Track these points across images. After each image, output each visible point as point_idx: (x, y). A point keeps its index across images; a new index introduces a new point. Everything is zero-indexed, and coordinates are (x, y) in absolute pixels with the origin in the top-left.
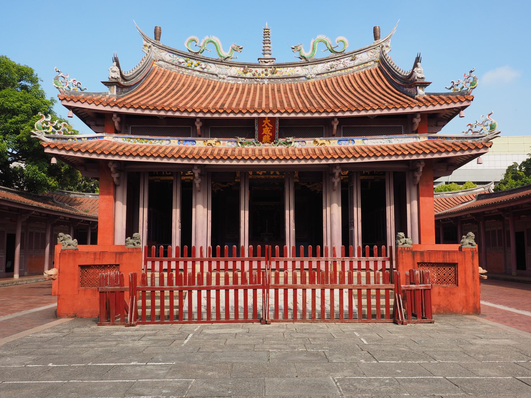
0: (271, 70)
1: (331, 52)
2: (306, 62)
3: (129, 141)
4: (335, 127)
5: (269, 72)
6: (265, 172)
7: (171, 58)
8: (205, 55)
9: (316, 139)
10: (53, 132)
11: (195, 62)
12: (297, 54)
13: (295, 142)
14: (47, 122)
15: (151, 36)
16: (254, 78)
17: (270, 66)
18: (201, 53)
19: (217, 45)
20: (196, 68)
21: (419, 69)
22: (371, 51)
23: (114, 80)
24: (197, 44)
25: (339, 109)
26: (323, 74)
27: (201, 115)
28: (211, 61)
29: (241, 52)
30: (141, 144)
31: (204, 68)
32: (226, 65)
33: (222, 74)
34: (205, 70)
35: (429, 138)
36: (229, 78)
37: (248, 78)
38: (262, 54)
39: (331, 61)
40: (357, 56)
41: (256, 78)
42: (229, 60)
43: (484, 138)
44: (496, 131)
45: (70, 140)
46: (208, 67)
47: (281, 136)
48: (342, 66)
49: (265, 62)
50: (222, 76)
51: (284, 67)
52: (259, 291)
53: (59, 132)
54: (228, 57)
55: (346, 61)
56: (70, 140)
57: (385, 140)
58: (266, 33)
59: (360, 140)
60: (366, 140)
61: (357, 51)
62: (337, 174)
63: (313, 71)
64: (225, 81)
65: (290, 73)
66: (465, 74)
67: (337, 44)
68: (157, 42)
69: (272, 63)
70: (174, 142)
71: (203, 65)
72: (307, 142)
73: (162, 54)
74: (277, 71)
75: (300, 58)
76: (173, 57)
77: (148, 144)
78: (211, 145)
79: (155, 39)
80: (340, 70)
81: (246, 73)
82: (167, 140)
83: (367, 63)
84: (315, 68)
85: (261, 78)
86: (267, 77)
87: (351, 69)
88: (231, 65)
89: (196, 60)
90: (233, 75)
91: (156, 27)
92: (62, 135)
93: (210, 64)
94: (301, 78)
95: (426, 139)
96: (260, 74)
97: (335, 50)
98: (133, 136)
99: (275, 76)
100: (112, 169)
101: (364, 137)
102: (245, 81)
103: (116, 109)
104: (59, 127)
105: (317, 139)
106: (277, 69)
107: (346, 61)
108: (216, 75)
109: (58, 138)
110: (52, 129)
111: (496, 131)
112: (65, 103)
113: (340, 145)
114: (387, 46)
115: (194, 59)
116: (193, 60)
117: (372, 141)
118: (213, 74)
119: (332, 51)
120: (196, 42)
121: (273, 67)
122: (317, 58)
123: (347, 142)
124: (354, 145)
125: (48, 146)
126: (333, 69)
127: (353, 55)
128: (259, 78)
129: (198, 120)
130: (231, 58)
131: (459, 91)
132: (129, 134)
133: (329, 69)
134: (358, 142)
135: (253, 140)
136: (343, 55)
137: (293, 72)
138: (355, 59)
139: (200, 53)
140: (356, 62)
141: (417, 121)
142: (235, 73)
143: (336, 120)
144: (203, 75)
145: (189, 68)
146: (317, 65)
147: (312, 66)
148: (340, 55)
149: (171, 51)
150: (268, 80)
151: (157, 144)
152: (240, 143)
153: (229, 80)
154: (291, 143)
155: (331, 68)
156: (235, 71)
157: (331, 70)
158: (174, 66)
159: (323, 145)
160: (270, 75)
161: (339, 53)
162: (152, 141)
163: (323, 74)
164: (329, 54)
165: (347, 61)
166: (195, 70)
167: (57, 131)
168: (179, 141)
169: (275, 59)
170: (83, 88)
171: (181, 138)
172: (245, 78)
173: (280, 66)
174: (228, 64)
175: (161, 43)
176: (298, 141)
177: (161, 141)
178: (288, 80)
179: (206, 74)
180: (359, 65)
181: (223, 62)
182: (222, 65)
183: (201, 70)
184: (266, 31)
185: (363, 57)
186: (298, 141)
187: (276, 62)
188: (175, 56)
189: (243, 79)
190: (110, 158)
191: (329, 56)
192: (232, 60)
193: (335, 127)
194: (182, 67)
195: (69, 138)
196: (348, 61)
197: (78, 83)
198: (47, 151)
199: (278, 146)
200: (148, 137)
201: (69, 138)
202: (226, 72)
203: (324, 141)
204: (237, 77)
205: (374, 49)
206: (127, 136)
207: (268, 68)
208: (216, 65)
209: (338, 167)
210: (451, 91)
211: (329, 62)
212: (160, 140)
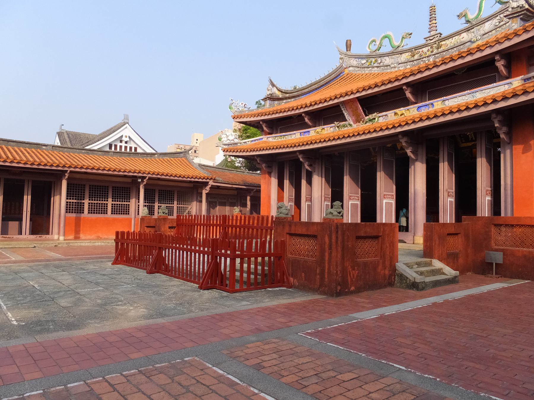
1: (500, 4)
2: (471, 26)
3: (275, 139)
6: (377, 150)
7: (357, 63)
8: (383, 51)
9: (395, 110)
11: (373, 60)
12: (463, 20)
13: (379, 117)
15: (344, 49)
17: (435, 43)
18: (378, 50)
19: (389, 38)
28: (385, 55)
29: (410, 37)
31: (380, 63)
32: (397, 54)
33: (393, 64)
37: (416, 60)
42: (400, 49)
46: (383, 60)
47: (366, 116)
49: (429, 39)
50: (393, 66)
56: (239, 144)
57: (469, 96)
58: (433, 11)
60: (447, 101)
63: (479, 33)
65: (455, 42)
68: (349, 53)
69: (437, 38)
72: (389, 115)
73: (351, 61)
74: (442, 45)
75: (466, 23)
76: (358, 61)
77: (285, 139)
81: (413, 56)
84: (482, 29)
85: (428, 57)
86: (433, 53)
88: (401, 53)
89: (374, 57)
90: (403, 62)
91: (347, 41)
93: (385, 58)
98: (276, 135)
101: (445, 98)
103: (259, 118)
105: (397, 111)
106: (443, 43)
108: (389, 65)
112: (238, 120)
115: (373, 57)
116: (372, 59)
118: (387, 66)
120: (375, 42)
121: (437, 42)
122: (484, 17)
123: (427, 107)
124: (435, 108)
126: (502, 23)
128: (425, 57)
130: (402, 46)
133: (497, 24)
134: (438, 105)
139: (377, 51)
141: (500, 64)
142: (405, 59)
144: (380, 69)
145: (370, 66)
150: (434, 56)
152: (338, 127)
154: (375, 119)
155: (500, 22)
156: (405, 57)
158: (359, 68)
159: (403, 116)
160: (435, 51)
162: (286, 136)
166: (374, 67)
168: (301, 133)
171: (301, 131)
173: (444, 39)
174: (398, 53)
175: (349, 53)
176: (382, 116)
178: (453, 50)
179: (382, 67)
182: (394, 55)
183: (378, 65)
188: (360, 60)
192: (404, 48)
197: (245, 105)
199: (366, 123)
204: (407, 62)
206: (273, 135)
207: (434, 44)
208: (389, 57)
209: (400, 136)
212: (290, 135)
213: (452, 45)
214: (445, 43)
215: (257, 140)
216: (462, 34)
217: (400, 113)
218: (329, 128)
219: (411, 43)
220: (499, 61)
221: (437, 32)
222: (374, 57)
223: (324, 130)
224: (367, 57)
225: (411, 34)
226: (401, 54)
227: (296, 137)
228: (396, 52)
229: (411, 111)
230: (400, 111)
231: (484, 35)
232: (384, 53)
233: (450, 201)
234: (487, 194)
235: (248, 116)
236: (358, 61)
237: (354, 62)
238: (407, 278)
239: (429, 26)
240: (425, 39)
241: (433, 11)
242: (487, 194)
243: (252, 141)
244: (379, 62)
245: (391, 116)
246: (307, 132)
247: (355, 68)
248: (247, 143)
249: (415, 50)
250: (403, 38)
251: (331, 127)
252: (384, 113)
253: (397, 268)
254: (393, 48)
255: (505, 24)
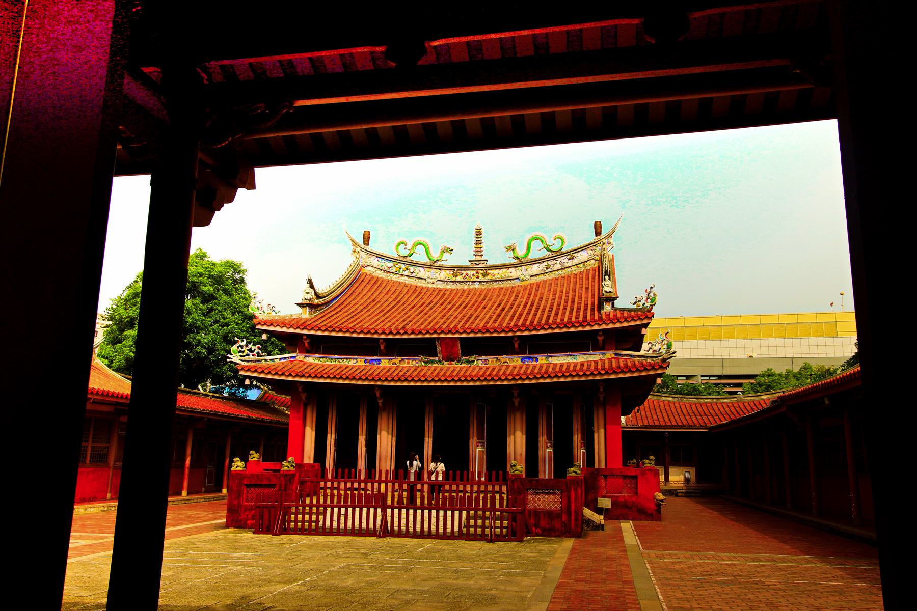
0: (482, 272)
2: (520, 263)
4: (516, 346)
5: (480, 275)
8: (414, 258)
10: (248, 355)
11: (403, 267)
13: (478, 360)
14: (242, 347)
15: (361, 241)
16: (464, 282)
20: (404, 273)
21: (606, 283)
22: (591, 248)
23: (308, 302)
24: (407, 247)
25: (517, 329)
26: (538, 275)
27: (383, 336)
30: (330, 363)
32: (435, 269)
34: (414, 275)
35: (616, 355)
36: (438, 282)
37: (458, 282)
38: (474, 255)
39: (547, 261)
40: (575, 255)
41: (467, 282)
42: (439, 263)
43: (661, 358)
44: (673, 350)
45: (263, 362)
46: (417, 271)
47: (462, 356)
48: (558, 266)
49: (475, 263)
50: (431, 281)
51: (496, 269)
52: (379, 510)
53: (253, 355)
54: (437, 260)
55: (564, 261)
56: (263, 362)
58: (479, 232)
59: (544, 358)
61: (583, 246)
62: (515, 395)
63: (527, 273)
64: (434, 286)
65: (503, 276)
66: (646, 290)
67: (554, 242)
70: (361, 361)
71: (412, 270)
72: (490, 360)
74: (489, 274)
75: (513, 258)
76: (380, 261)
78: (395, 363)
79: (364, 244)
80: (557, 270)
81: (456, 276)
82: (354, 359)
83: (587, 262)
86: (478, 280)
87: (569, 269)
88: (441, 268)
91: (365, 231)
92: (256, 358)
94: (515, 281)
95: (613, 356)
96: (470, 277)
97: (551, 248)
99: (486, 278)
100: (300, 390)
102: (455, 285)
103: (305, 332)
104: (253, 350)
106: (489, 272)
107: (564, 261)
108: (425, 279)
109: (252, 361)
110: (246, 352)
111: (673, 350)
113: (523, 363)
114: (609, 243)
116: (401, 265)
117: (556, 358)
119: (549, 250)
120: (406, 245)
121: (484, 269)
125: (242, 369)
127: (571, 254)
128: (469, 282)
129: (381, 341)
131: (641, 307)
132: (319, 354)
134: (542, 360)
135: (436, 358)
136: (559, 254)
137: (506, 274)
138: (572, 259)
140: (575, 261)
143: (516, 339)
146: (531, 266)
147: (527, 267)
148: (556, 254)
149: (380, 256)
151: (344, 364)
152: (424, 362)
153: (438, 284)
154: (474, 361)
155: (547, 268)
156: (444, 275)
157: (547, 271)
158: (382, 271)
160: (481, 278)
161: (556, 251)
162: (340, 360)
163: (538, 275)
164: (545, 253)
165: (564, 260)
166: (403, 275)
167: (251, 354)
168: (366, 360)
169: (487, 261)
170: (276, 311)
171: (367, 357)
172: (455, 282)
175: (371, 247)
176: (481, 360)
177: (349, 360)
179: (414, 279)
180: (578, 264)
181: (433, 265)
182: (431, 268)
183: (410, 275)
184: (477, 231)
185: (583, 256)
186: (481, 360)
187: (490, 263)
188: (383, 261)
189: (453, 283)
190: (297, 379)
191: (544, 255)
193: (516, 346)
194: (390, 272)
195: (262, 360)
196: (566, 260)
198: (242, 373)
199: (461, 364)
200: (336, 356)
201: (262, 360)
202: (435, 276)
203: (507, 360)
205: (595, 246)
206: (317, 355)
210: (635, 307)
211: (545, 261)
213: (499, 276)
214: (492, 272)
215: (288, 358)
216: (510, 269)
217: (503, 360)
218: (411, 361)
219: (451, 260)
220: (601, 336)
221: (483, 258)
222: (404, 264)
223: (403, 362)
224: (395, 261)
225: (453, 250)
226: (440, 269)
227: (357, 364)
228: (433, 265)
229: (515, 360)
230: (503, 358)
231: (532, 276)
232: (419, 263)
233: (548, 451)
234: (581, 447)
235: (284, 324)
236: (380, 261)
237: (375, 261)
238: (594, 522)
239: (475, 249)
240: (469, 261)
241: (479, 232)
242: (581, 447)
243: (280, 359)
244: (412, 271)
245: (492, 362)
246: (375, 360)
247: (376, 269)
248: (275, 360)
249: (458, 270)
250: (443, 251)
251: (413, 360)
252: (484, 357)
253: (584, 514)
254: (430, 259)
255: (552, 272)
